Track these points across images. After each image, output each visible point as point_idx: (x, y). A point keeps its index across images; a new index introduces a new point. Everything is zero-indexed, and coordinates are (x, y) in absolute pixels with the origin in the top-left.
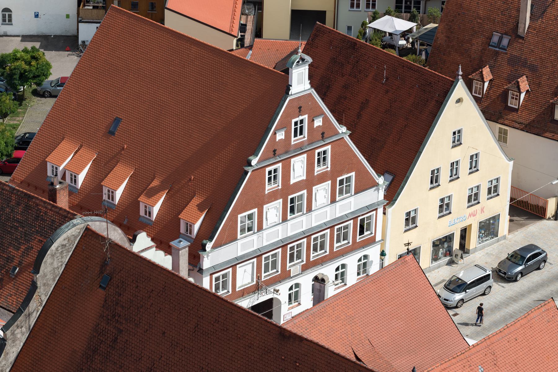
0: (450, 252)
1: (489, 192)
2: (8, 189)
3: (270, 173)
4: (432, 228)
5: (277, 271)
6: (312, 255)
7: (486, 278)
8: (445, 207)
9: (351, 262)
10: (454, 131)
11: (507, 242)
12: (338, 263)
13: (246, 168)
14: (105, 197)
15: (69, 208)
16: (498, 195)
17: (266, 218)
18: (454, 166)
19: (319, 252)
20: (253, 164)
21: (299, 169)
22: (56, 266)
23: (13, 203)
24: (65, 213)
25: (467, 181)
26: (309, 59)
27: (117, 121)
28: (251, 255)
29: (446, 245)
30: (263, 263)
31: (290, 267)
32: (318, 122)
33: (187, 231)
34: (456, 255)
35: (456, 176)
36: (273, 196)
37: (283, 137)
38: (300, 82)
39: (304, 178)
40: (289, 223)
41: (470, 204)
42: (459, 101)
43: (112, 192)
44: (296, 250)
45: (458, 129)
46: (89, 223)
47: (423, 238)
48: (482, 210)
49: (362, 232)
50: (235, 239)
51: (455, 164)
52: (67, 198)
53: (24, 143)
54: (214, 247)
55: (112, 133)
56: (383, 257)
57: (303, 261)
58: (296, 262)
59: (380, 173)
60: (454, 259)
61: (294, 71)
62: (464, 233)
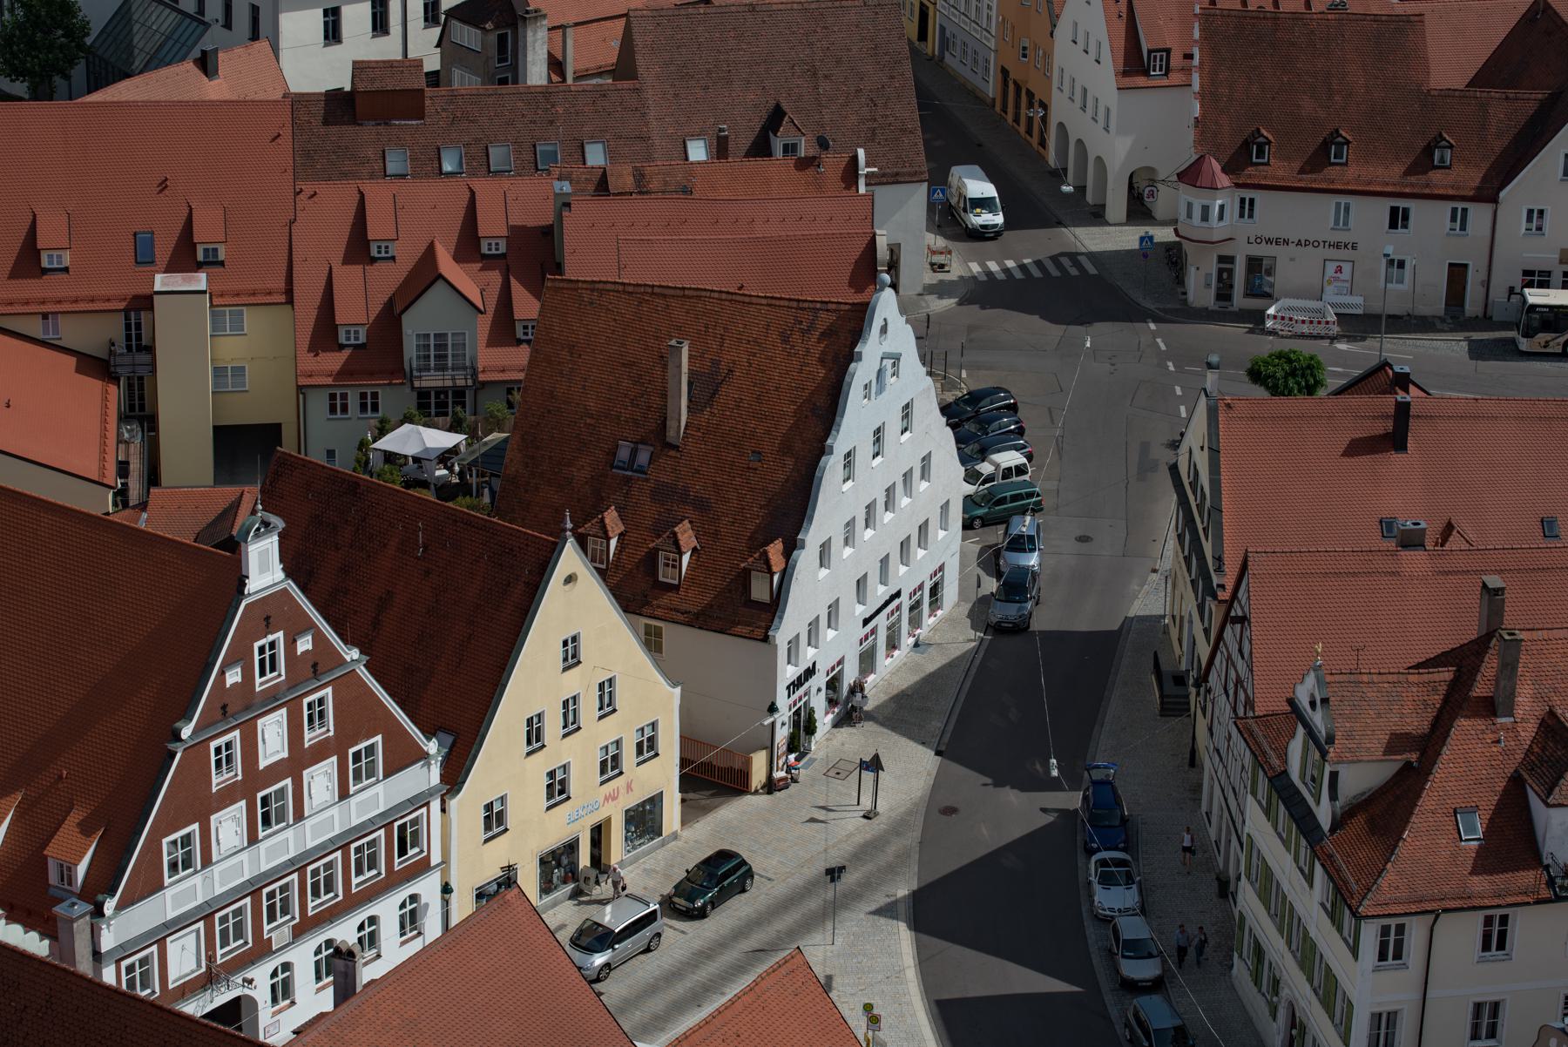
1: (640, 751)
4: (537, 830)
6: (310, 905)
7: (650, 918)
9: (387, 909)
11: (680, 843)
12: (362, 915)
13: (171, 746)
16: (657, 755)
18: (570, 708)
19: (324, 898)
25: (597, 734)
26: (278, 523)
31: (270, 931)
32: (304, 644)
34: (587, 879)
36: (227, 797)
38: (264, 568)
39: (285, 755)
40: (263, 846)
41: (605, 777)
42: (570, 579)
44: (278, 897)
47: (523, 848)
48: (629, 788)
49: (403, 851)
50: (161, 887)
54: (121, 907)
57: (293, 918)
58: (280, 921)
59: (429, 733)
60: (583, 886)
61: (251, 548)
62: (599, 834)
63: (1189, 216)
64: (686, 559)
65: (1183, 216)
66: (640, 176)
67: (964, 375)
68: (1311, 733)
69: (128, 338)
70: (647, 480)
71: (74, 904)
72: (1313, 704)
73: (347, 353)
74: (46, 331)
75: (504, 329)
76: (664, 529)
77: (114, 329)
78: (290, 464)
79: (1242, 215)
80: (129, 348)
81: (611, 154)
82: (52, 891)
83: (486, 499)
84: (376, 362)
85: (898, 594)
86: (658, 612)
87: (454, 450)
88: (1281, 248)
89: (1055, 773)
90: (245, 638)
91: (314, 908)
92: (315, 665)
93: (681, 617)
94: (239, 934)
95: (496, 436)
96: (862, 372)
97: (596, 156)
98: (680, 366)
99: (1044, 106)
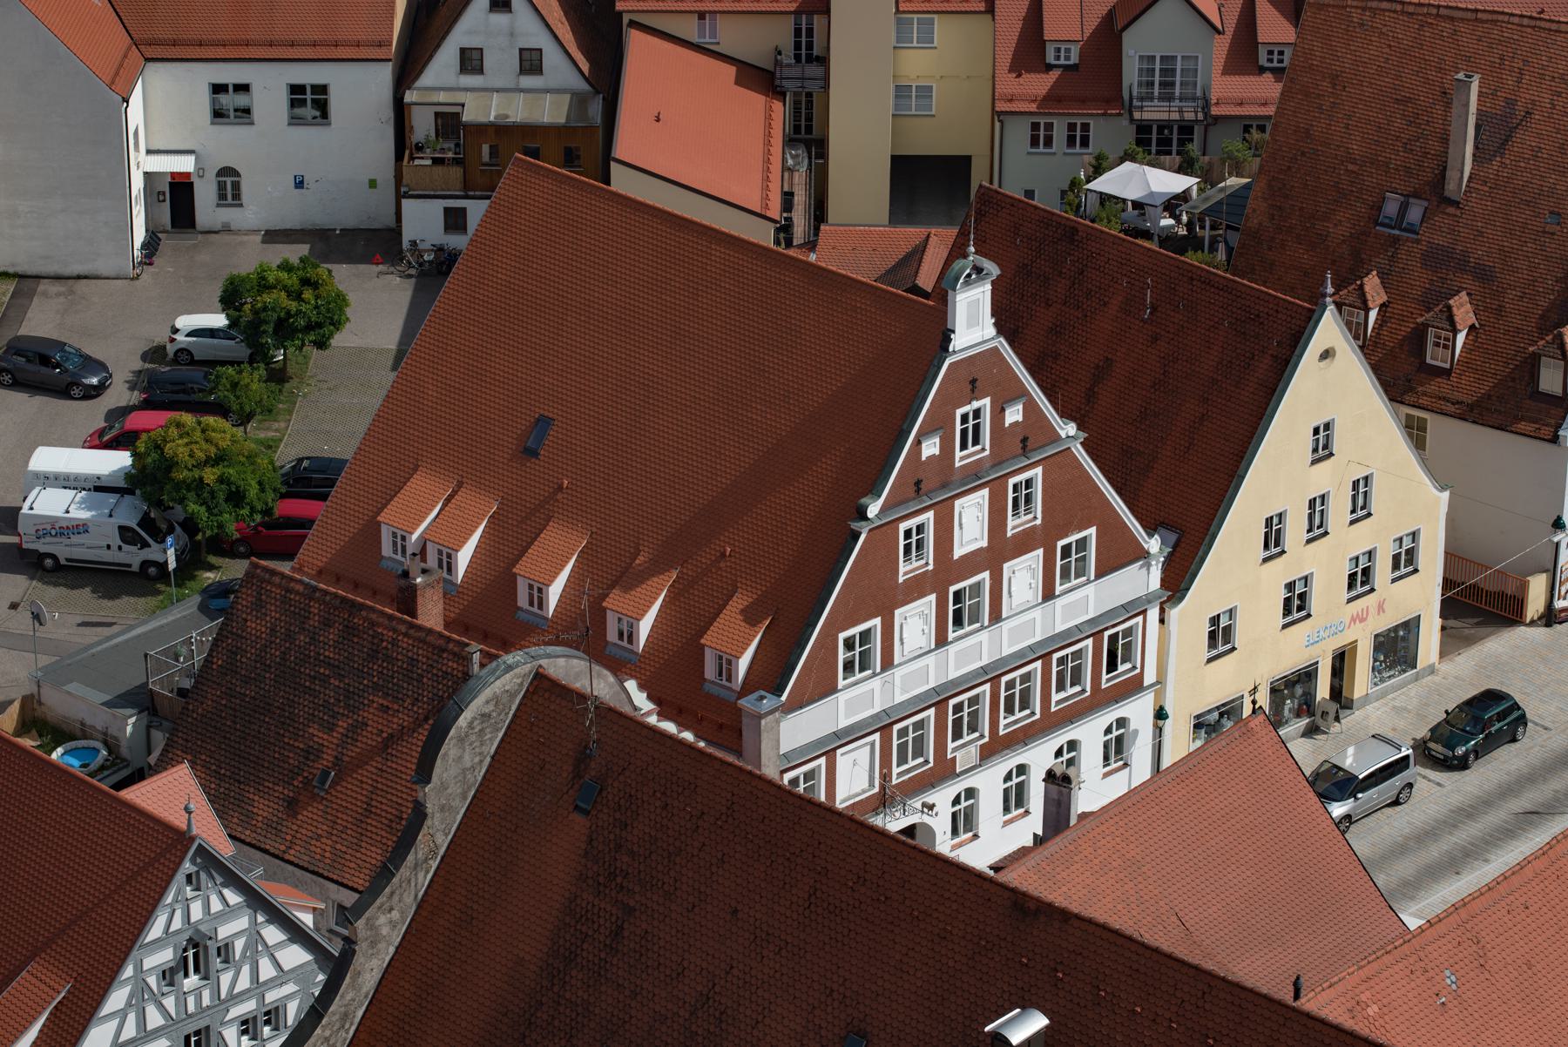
0: (1309, 707)
1: (1396, 566)
2: (301, 588)
3: (908, 534)
4: (1269, 651)
5: (927, 762)
6: (1003, 722)
7: (1401, 765)
8: (1296, 602)
9: (1090, 733)
10: (1315, 424)
11: (1437, 679)
12: (1061, 738)
13: (855, 525)
14: (522, 601)
15: (447, 625)
16: (1416, 571)
17: (901, 639)
18: (1317, 506)
19: (1019, 715)
20: (870, 515)
21: (971, 522)
22: (468, 765)
23: (314, 622)
24: (441, 642)
26: (993, 269)
27: (543, 423)
28: (870, 725)
29: (1299, 690)
30: (895, 743)
31: (955, 750)
32: (1014, 414)
33: (720, 674)
34: (1324, 714)
35: (1321, 531)
36: (915, 589)
37: (936, 451)
38: (973, 322)
39: (984, 543)
41: (1354, 593)
42: (1327, 355)
43: (540, 590)
44: (966, 710)
45: (1326, 420)
46: (543, 662)
48: (1381, 608)
49: (1112, 666)
50: (833, 690)
51: (1318, 502)
52: (441, 606)
53: (312, 480)
55: (532, 453)
56: (1160, 723)
57: (982, 736)
58: (967, 738)
59: (1151, 529)
60: (1319, 721)
61: (959, 298)
62: (1342, 662)
64: (1461, 338)
69: (797, 46)
70: (1418, 242)
71: (762, 698)
73: (1054, 75)
74: (702, 34)
75: (1245, 53)
76: (1437, 301)
77: (780, 34)
78: (991, 200)
80: (798, 58)
82: (707, 687)
83: (1221, 255)
84: (1090, 88)
86: (1424, 401)
87: (1184, 196)
90: (948, 402)
91: (1007, 726)
92: (1024, 440)
93: (1451, 408)
94: (919, 751)
95: (1234, 182)
98: (1467, 105)
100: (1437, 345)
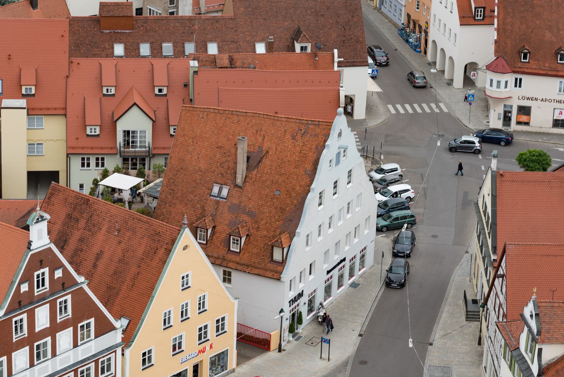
3: (16, 322)
26: (47, 216)
32: (58, 274)
36: (20, 344)
37: (27, 289)
39: (48, 325)
42: (185, 248)
62: (196, 368)
63: (491, 85)
65: (488, 86)
66: (231, 60)
67: (382, 157)
68: (530, 330)
72: (531, 316)
79: (516, 86)
81: (220, 49)
85: (344, 260)
88: (534, 102)
89: (411, 345)
90: (30, 270)
92: (63, 284)
96: (327, 155)
97: (213, 49)
99: (426, 33)
100: (234, 243)
